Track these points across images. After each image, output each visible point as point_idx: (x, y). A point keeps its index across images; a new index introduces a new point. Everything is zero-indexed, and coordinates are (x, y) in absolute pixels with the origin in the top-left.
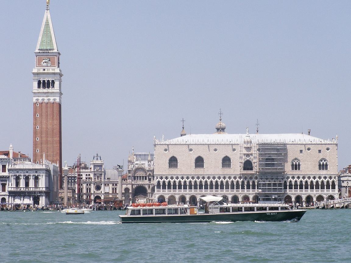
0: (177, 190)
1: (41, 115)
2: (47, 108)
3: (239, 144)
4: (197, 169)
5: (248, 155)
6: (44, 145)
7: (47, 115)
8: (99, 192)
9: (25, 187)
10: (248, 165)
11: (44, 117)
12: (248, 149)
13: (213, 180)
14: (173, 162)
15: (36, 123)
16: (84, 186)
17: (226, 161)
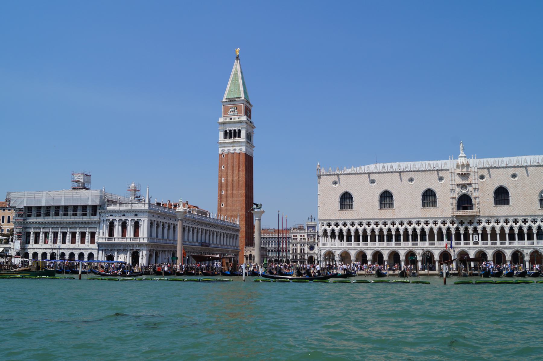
0: (353, 242)
1: (227, 167)
2: (233, 158)
3: (448, 170)
4: (383, 211)
5: (464, 186)
6: (230, 199)
7: (233, 167)
8: (313, 252)
9: (120, 237)
10: (465, 202)
11: (230, 168)
12: (464, 176)
13: (408, 226)
14: (346, 200)
15: (221, 176)
16: (299, 246)
17: (429, 197)
